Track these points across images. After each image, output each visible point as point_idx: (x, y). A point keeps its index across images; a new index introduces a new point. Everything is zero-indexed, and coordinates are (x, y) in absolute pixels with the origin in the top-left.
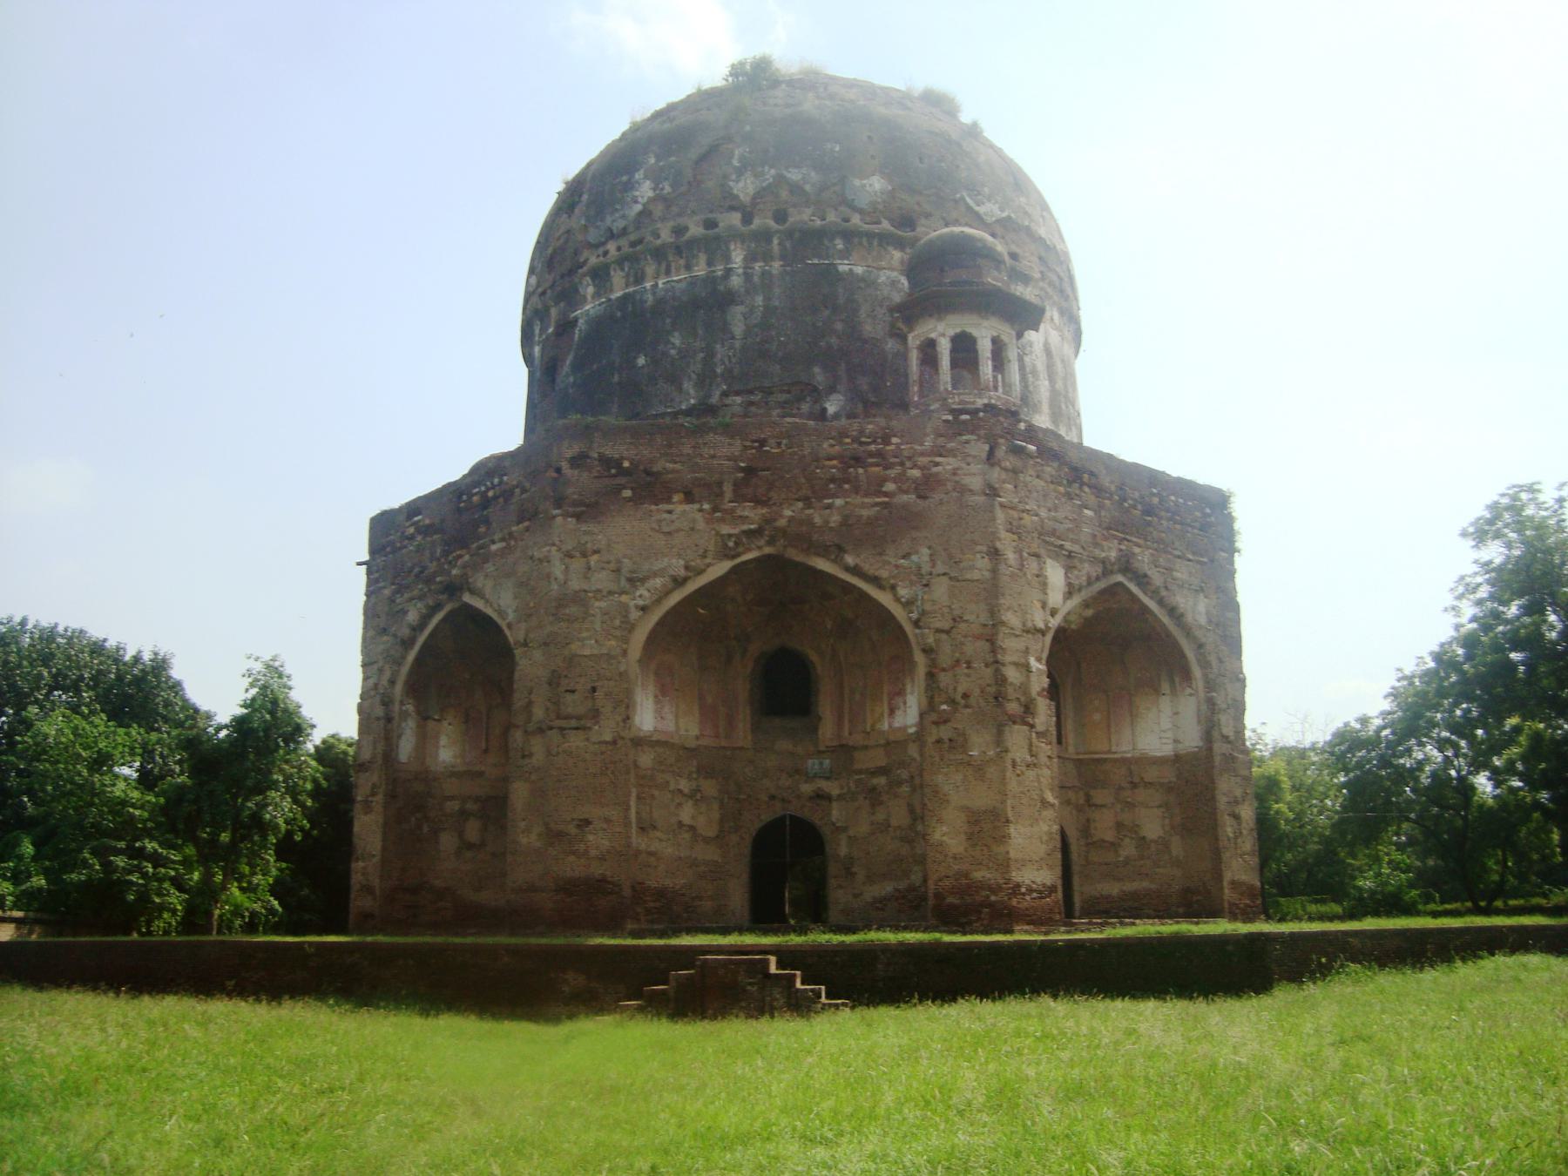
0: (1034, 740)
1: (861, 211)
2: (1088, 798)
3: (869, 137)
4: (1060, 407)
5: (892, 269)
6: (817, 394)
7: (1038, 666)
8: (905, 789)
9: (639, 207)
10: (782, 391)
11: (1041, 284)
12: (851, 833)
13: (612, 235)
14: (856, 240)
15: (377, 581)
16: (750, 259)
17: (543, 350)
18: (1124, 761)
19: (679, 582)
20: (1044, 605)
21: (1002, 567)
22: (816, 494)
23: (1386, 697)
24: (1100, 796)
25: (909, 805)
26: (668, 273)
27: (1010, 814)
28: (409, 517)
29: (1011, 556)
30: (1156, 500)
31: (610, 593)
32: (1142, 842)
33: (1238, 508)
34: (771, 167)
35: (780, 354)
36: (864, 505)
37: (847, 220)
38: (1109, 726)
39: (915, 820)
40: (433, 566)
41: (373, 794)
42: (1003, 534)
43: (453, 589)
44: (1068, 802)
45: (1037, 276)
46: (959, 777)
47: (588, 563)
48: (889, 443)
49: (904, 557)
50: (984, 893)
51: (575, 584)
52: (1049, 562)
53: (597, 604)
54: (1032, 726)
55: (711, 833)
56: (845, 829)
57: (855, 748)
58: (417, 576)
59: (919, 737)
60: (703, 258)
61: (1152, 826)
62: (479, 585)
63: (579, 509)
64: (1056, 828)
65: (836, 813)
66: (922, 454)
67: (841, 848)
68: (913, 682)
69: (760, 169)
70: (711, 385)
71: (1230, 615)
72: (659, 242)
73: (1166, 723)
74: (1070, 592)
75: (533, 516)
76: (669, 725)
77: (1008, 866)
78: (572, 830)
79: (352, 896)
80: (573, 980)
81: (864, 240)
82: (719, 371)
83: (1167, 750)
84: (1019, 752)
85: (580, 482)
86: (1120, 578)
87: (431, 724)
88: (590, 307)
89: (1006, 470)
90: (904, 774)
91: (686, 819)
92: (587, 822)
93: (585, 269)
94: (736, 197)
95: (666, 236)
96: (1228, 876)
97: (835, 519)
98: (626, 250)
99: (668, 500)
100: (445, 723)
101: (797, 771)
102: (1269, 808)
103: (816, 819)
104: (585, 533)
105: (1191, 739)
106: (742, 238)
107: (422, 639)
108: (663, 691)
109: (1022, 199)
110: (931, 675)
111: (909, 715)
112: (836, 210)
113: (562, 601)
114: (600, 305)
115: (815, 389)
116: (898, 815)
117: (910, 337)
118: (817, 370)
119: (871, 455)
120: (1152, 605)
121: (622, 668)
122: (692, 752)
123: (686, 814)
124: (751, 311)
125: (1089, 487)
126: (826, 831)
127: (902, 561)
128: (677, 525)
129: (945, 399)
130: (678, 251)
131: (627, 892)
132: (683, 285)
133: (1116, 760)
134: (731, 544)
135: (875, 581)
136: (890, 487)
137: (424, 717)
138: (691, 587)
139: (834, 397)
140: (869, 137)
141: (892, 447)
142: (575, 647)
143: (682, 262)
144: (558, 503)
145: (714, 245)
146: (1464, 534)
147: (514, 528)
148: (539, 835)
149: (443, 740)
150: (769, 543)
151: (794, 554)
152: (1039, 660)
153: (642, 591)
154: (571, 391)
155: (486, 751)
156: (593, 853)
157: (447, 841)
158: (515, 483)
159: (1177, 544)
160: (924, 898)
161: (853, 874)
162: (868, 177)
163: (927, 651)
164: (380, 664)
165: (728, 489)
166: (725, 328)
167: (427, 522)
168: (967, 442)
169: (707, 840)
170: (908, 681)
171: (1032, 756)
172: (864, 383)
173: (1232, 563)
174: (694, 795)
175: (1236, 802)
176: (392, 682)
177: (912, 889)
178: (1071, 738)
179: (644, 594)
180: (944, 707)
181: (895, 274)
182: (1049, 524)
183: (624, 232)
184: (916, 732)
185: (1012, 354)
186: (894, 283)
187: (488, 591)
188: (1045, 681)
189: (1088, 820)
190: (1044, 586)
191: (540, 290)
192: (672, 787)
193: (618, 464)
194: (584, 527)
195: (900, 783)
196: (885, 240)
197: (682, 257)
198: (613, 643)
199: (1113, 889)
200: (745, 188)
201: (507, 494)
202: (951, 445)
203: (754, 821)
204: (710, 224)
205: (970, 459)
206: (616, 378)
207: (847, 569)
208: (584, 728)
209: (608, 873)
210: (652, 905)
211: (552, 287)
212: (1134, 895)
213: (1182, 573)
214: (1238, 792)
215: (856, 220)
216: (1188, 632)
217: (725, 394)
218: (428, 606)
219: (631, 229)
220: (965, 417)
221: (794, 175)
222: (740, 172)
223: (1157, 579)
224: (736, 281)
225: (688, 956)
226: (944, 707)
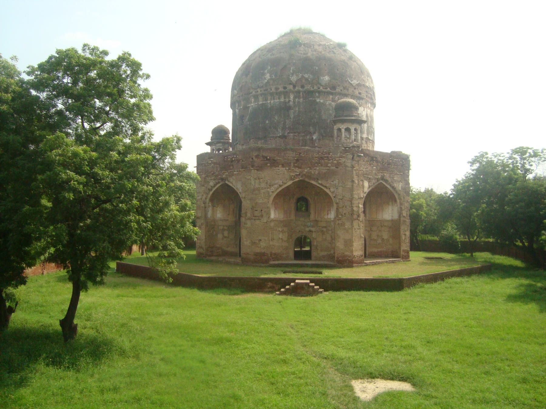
0: (360, 224)
1: (322, 86)
2: (371, 229)
3: (325, 64)
4: (369, 130)
5: (330, 101)
6: (311, 134)
7: (361, 206)
8: (330, 232)
9: (266, 81)
10: (303, 133)
11: (367, 99)
13: (259, 87)
14: (321, 93)
15: (200, 172)
16: (295, 97)
17: (239, 111)
18: (380, 220)
19: (280, 186)
20: (363, 192)
21: (354, 184)
23: (453, 185)
24: (374, 229)
25: (331, 236)
27: (354, 241)
28: (210, 158)
29: (356, 182)
31: (265, 188)
33: (411, 159)
34: (300, 73)
35: (302, 124)
37: (319, 88)
38: (377, 213)
39: (332, 239)
40: (217, 173)
41: (202, 225)
43: (222, 179)
45: (365, 97)
47: (260, 181)
48: (330, 155)
49: (332, 182)
50: (347, 257)
51: (257, 186)
52: (365, 181)
53: (262, 191)
54: (359, 220)
58: (213, 174)
59: (334, 221)
60: (283, 96)
61: (385, 236)
62: (231, 180)
63: (257, 168)
64: (364, 242)
65: (314, 235)
66: (337, 157)
68: (333, 209)
69: (297, 74)
70: (285, 130)
71: (407, 186)
72: (271, 91)
73: (390, 211)
74: (369, 187)
75: (246, 168)
76: (278, 217)
77: (353, 251)
78: (257, 242)
80: (270, 284)
81: (323, 93)
82: (287, 127)
85: (258, 162)
86: (381, 181)
87: (215, 208)
88: (253, 105)
89: (356, 161)
90: (330, 229)
91: (281, 237)
92: (260, 240)
93: (251, 95)
94: (292, 81)
95: (273, 90)
96: (402, 250)
97: (317, 172)
98: (263, 92)
99: (278, 167)
100: (219, 208)
102: (419, 213)
104: (259, 174)
105: (396, 216)
106: (293, 92)
107: (214, 189)
108: (276, 208)
109: (363, 76)
110: (337, 209)
111: (332, 215)
112: (316, 85)
114: (256, 105)
115: (311, 133)
116: (329, 238)
118: (311, 128)
119: (325, 157)
120: (388, 186)
121: (268, 206)
123: (281, 236)
125: (375, 161)
129: (343, 144)
130: (277, 94)
132: (278, 103)
133: (377, 220)
135: (326, 187)
136: (329, 165)
137: (213, 206)
138: (283, 187)
139: (315, 135)
140: (325, 64)
141: (330, 155)
143: (277, 97)
144: (253, 166)
145: (286, 94)
146: (468, 162)
147: (241, 170)
149: (218, 212)
150: (302, 177)
151: (307, 180)
152: (361, 204)
153: (272, 188)
154: (248, 126)
155: (229, 215)
156: (262, 247)
157: (220, 236)
158: (240, 158)
159: (395, 171)
160: (334, 257)
161: (318, 249)
162: (324, 76)
163: (337, 203)
164: (203, 194)
165: (292, 164)
166: (289, 116)
167: (215, 161)
168: (348, 155)
170: (332, 208)
171: (359, 226)
172: (322, 131)
173: (408, 172)
174: (282, 232)
175: (405, 231)
176: (206, 198)
178: (367, 215)
180: (340, 216)
181: (330, 102)
183: (262, 87)
185: (359, 132)
186: (330, 104)
187: (234, 183)
188: (363, 209)
189: (371, 234)
190: (363, 187)
191: (238, 95)
192: (278, 230)
193: (266, 158)
197: (277, 95)
198: (266, 200)
199: (375, 250)
200: (294, 79)
201: (238, 161)
203: (295, 237)
204: (285, 88)
205: (348, 159)
206: (260, 125)
207: (319, 184)
210: (273, 257)
211: (242, 96)
212: (381, 252)
214: (406, 229)
215: (321, 88)
216: (397, 192)
217: (289, 133)
221: (306, 76)
222: (293, 74)
223: (390, 180)
224: (291, 103)
226: (340, 216)
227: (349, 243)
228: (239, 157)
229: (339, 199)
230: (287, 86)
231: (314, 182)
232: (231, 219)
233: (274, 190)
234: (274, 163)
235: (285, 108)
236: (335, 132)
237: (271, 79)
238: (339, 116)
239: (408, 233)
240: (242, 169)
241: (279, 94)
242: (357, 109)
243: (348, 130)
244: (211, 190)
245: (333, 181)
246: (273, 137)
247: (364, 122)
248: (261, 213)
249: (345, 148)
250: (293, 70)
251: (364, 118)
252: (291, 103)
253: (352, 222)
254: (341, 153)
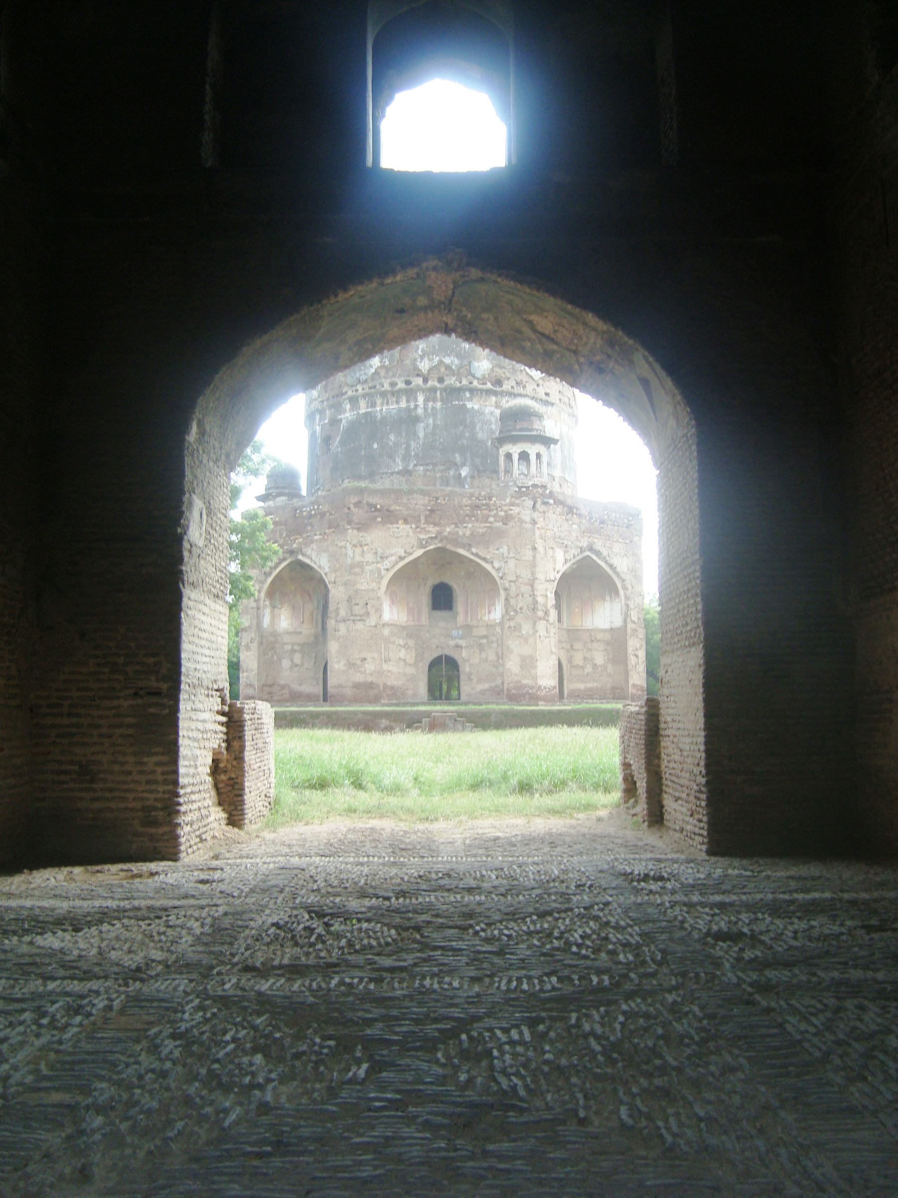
1: (478, 379)
2: (572, 646)
6: (457, 467)
7: (551, 595)
8: (495, 645)
9: (373, 370)
12: (471, 662)
13: (359, 381)
16: (426, 400)
18: (588, 630)
19: (401, 558)
20: (554, 569)
21: (537, 555)
22: (460, 521)
24: (577, 646)
26: (388, 404)
29: (541, 549)
30: (606, 517)
32: (595, 666)
36: (481, 528)
37: (471, 383)
42: (538, 540)
43: (292, 552)
44: (563, 648)
46: (518, 642)
49: (498, 549)
51: (358, 558)
54: (548, 621)
55: (412, 661)
56: (468, 660)
57: (473, 626)
59: (501, 624)
60: (404, 399)
61: (600, 659)
62: (309, 552)
64: (557, 662)
65: (464, 654)
66: (505, 505)
67: (465, 668)
76: (396, 618)
78: (359, 662)
79: (241, 688)
80: (384, 722)
82: (413, 454)
83: (607, 626)
84: (542, 631)
85: (359, 514)
86: (588, 553)
88: (348, 415)
90: (495, 639)
91: (402, 657)
92: (365, 659)
93: (346, 397)
95: (387, 387)
96: (631, 682)
97: (468, 533)
98: (367, 390)
99: (397, 523)
101: (448, 636)
103: (456, 657)
105: (618, 622)
106: (423, 391)
108: (393, 602)
110: (506, 599)
111: (497, 614)
113: (352, 566)
116: (492, 656)
117: (501, 450)
118: (457, 455)
119: (484, 505)
120: (603, 564)
122: (404, 628)
124: (427, 426)
126: (460, 662)
127: (497, 552)
128: (401, 534)
130: (393, 393)
131: (381, 688)
135: (484, 559)
136: (491, 519)
137: (273, 607)
139: (464, 468)
142: (359, 586)
143: (394, 399)
144: (350, 522)
145: (410, 393)
148: (345, 665)
149: (283, 617)
151: (450, 547)
153: (386, 562)
156: (368, 672)
157: (286, 663)
163: (506, 589)
165: (422, 518)
166: (415, 434)
169: (410, 665)
172: (478, 461)
177: (496, 686)
179: (387, 563)
180: (512, 613)
181: (492, 409)
182: (557, 534)
183: (366, 381)
184: (500, 623)
185: (545, 459)
188: (554, 602)
193: (375, 507)
194: (361, 534)
195: (493, 642)
196: (489, 392)
199: (581, 686)
201: (323, 515)
202: (518, 501)
203: (429, 657)
204: (408, 383)
206: (363, 452)
207: (473, 554)
208: (363, 620)
209: (374, 681)
211: (328, 399)
212: (591, 689)
213: (617, 548)
215: (475, 383)
216: (618, 574)
217: (415, 465)
218: (279, 559)
219: (369, 380)
220: (524, 489)
221: (447, 360)
222: (422, 357)
223: (605, 552)
225: (428, 714)
226: (512, 613)
227: (528, 663)
228: (325, 508)
230: (411, 379)
231: (462, 551)
232: (308, 630)
233: (390, 567)
234: (389, 517)
235: (409, 420)
236: (502, 459)
237: (382, 367)
238: (508, 431)
239: (642, 654)
240: (329, 528)
241: (396, 394)
242: (540, 417)
243: (524, 456)
244: (270, 573)
245: (498, 549)
246: (386, 473)
247: (555, 442)
248: (364, 610)
249: (520, 488)
250: (423, 350)
251: (556, 437)
252: (420, 411)
253: (535, 624)
254: (512, 497)
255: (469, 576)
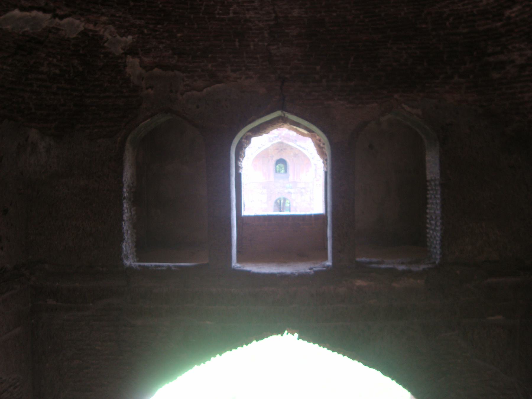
19: (259, 148)
65: (293, 196)
110: (316, 170)
134: (271, 139)
135: (304, 148)
151: (285, 142)
163: (315, 165)
203: (274, 199)
207: (298, 145)
229: (318, 160)
231: (291, 144)
255: (296, 155)
